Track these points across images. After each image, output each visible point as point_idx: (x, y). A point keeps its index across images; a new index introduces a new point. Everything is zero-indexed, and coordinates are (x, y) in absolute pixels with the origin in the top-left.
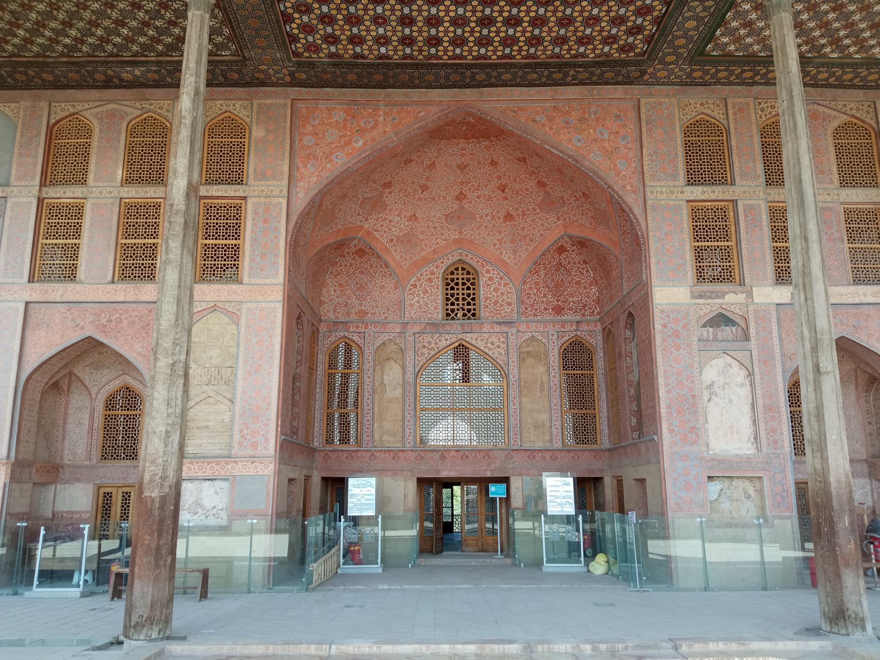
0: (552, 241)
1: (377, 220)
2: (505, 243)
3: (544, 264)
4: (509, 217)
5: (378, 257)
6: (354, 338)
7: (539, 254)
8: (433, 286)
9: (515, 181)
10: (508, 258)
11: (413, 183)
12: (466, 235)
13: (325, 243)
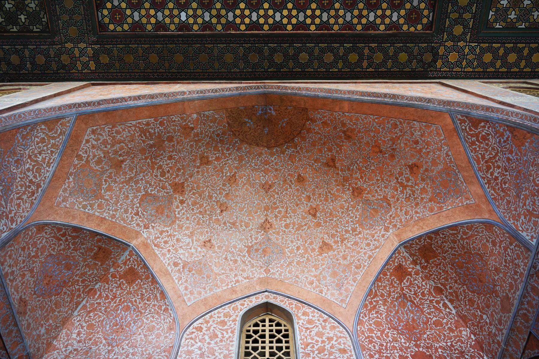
0: (386, 257)
1: (161, 233)
2: (325, 278)
3: (382, 295)
4: (325, 247)
5: (154, 281)
7: (372, 279)
8: (226, 330)
9: (326, 200)
10: (331, 295)
11: (210, 197)
12: (274, 274)
13: (75, 223)
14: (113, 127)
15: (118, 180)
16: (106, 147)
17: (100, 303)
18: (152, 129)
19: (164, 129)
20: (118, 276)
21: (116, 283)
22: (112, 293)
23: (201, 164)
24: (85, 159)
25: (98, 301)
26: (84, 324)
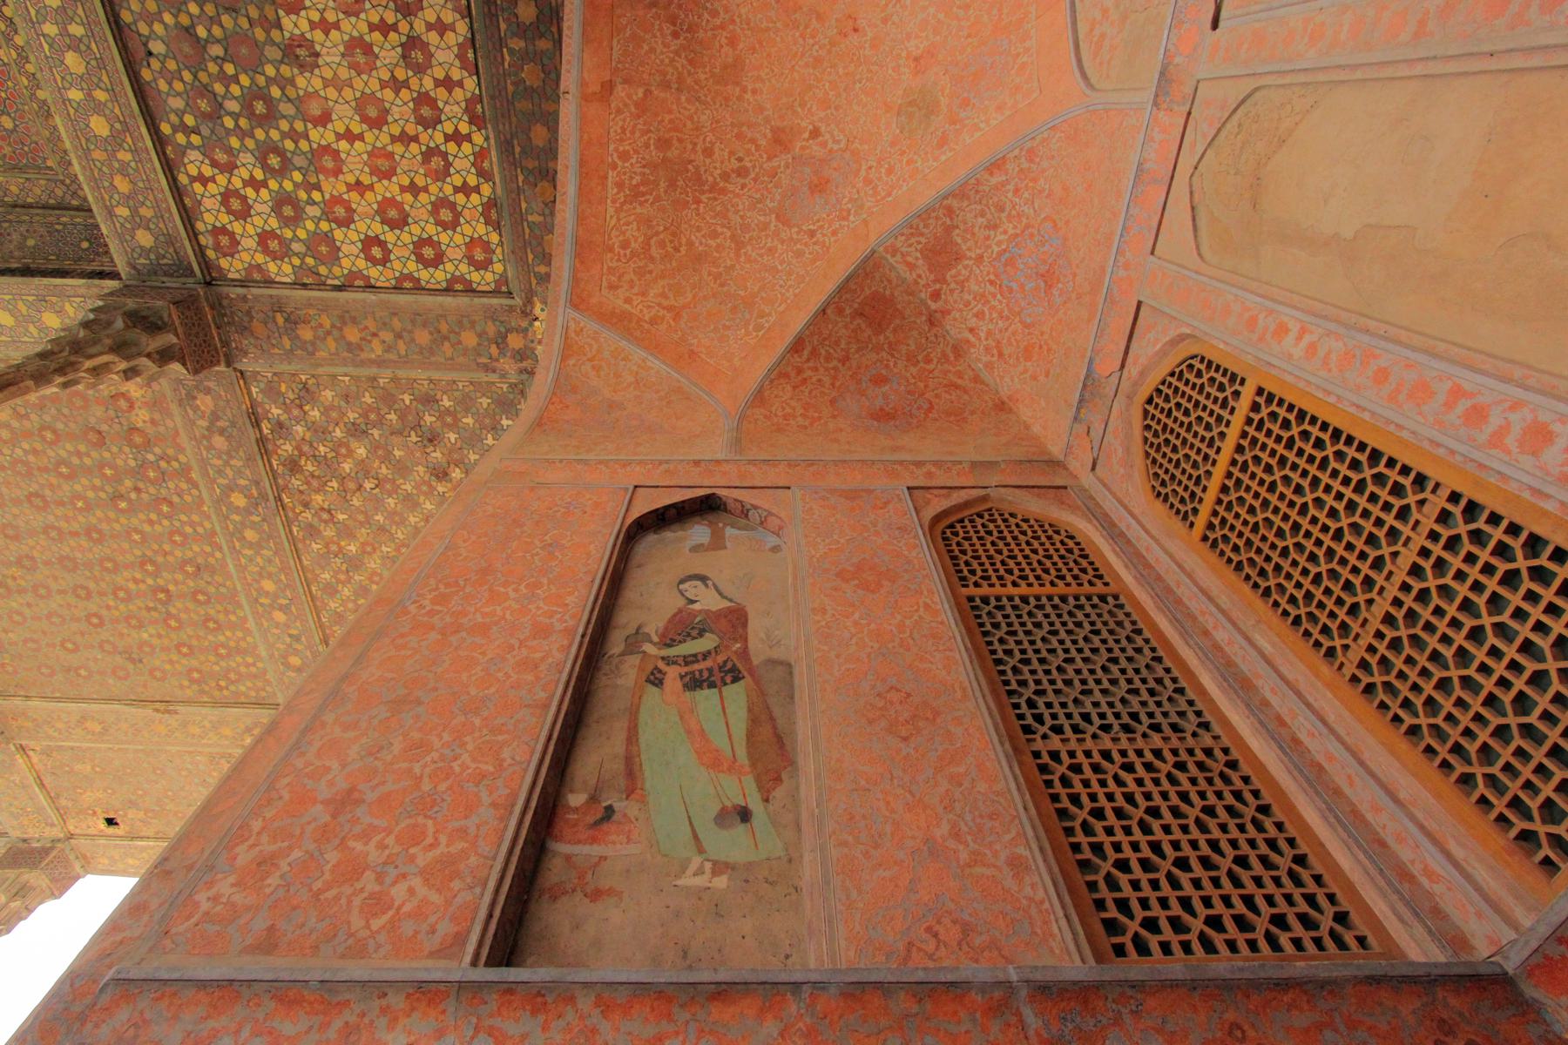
1: (867, 181)
6: (1143, 360)
14: (611, 250)
15: (729, 263)
16: (650, 272)
17: (989, 333)
18: (631, 178)
19: (636, 152)
20: (938, 286)
21: (952, 291)
22: (973, 303)
23: (737, 84)
24: (662, 313)
25: (983, 335)
26: (1021, 368)
